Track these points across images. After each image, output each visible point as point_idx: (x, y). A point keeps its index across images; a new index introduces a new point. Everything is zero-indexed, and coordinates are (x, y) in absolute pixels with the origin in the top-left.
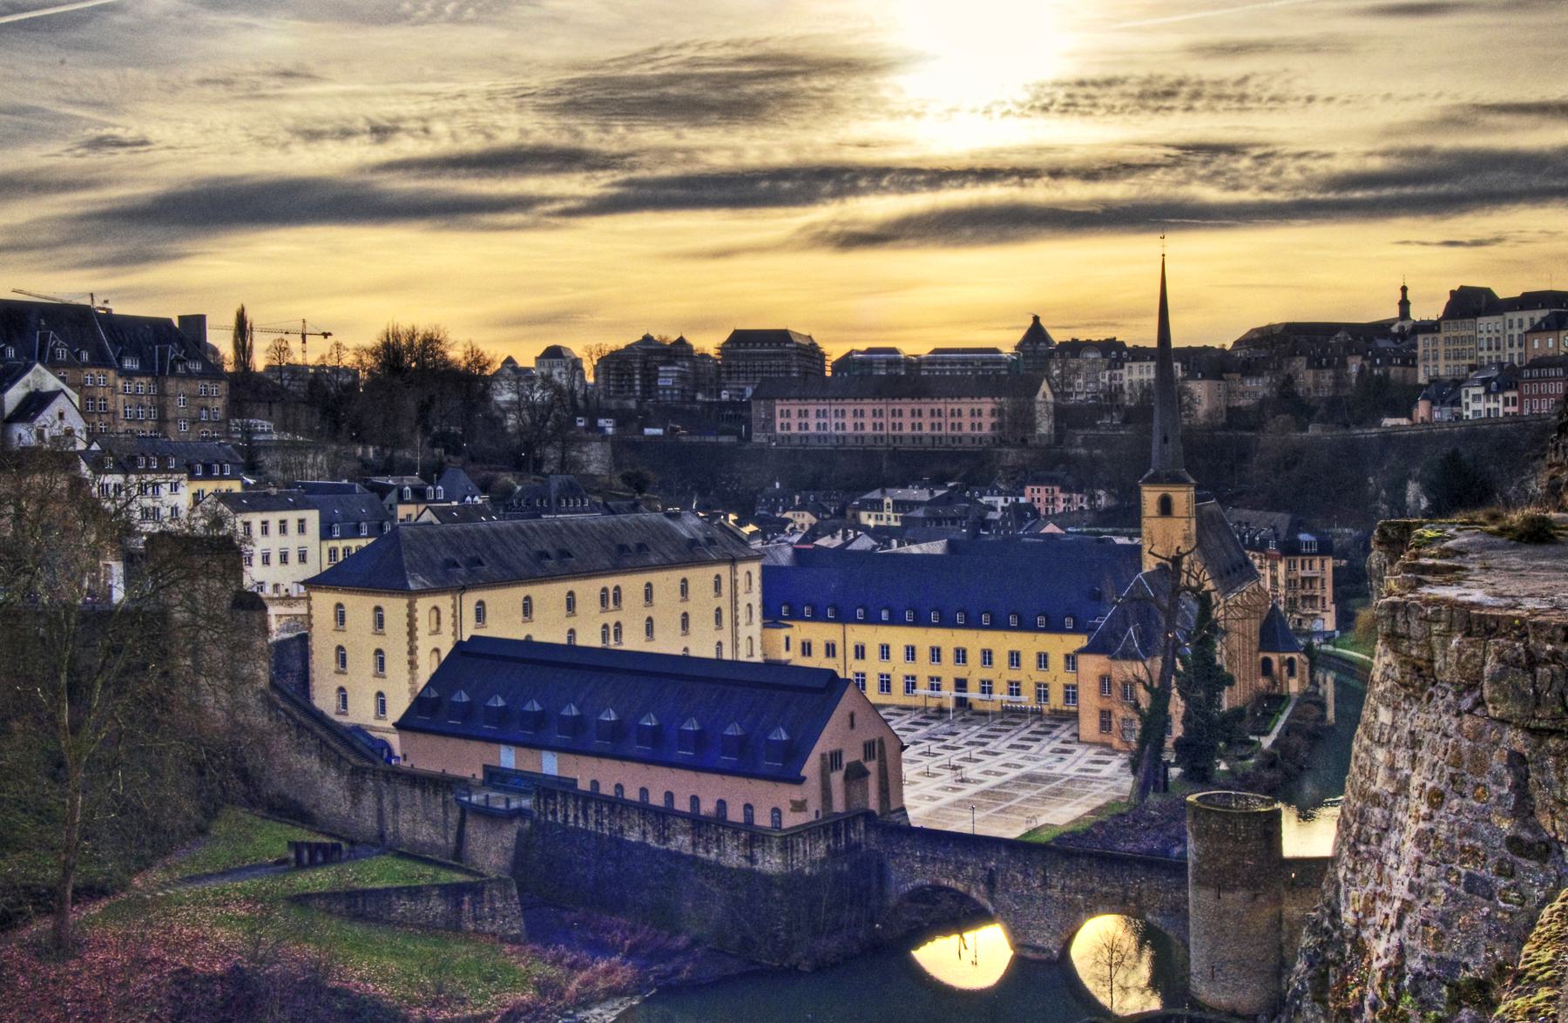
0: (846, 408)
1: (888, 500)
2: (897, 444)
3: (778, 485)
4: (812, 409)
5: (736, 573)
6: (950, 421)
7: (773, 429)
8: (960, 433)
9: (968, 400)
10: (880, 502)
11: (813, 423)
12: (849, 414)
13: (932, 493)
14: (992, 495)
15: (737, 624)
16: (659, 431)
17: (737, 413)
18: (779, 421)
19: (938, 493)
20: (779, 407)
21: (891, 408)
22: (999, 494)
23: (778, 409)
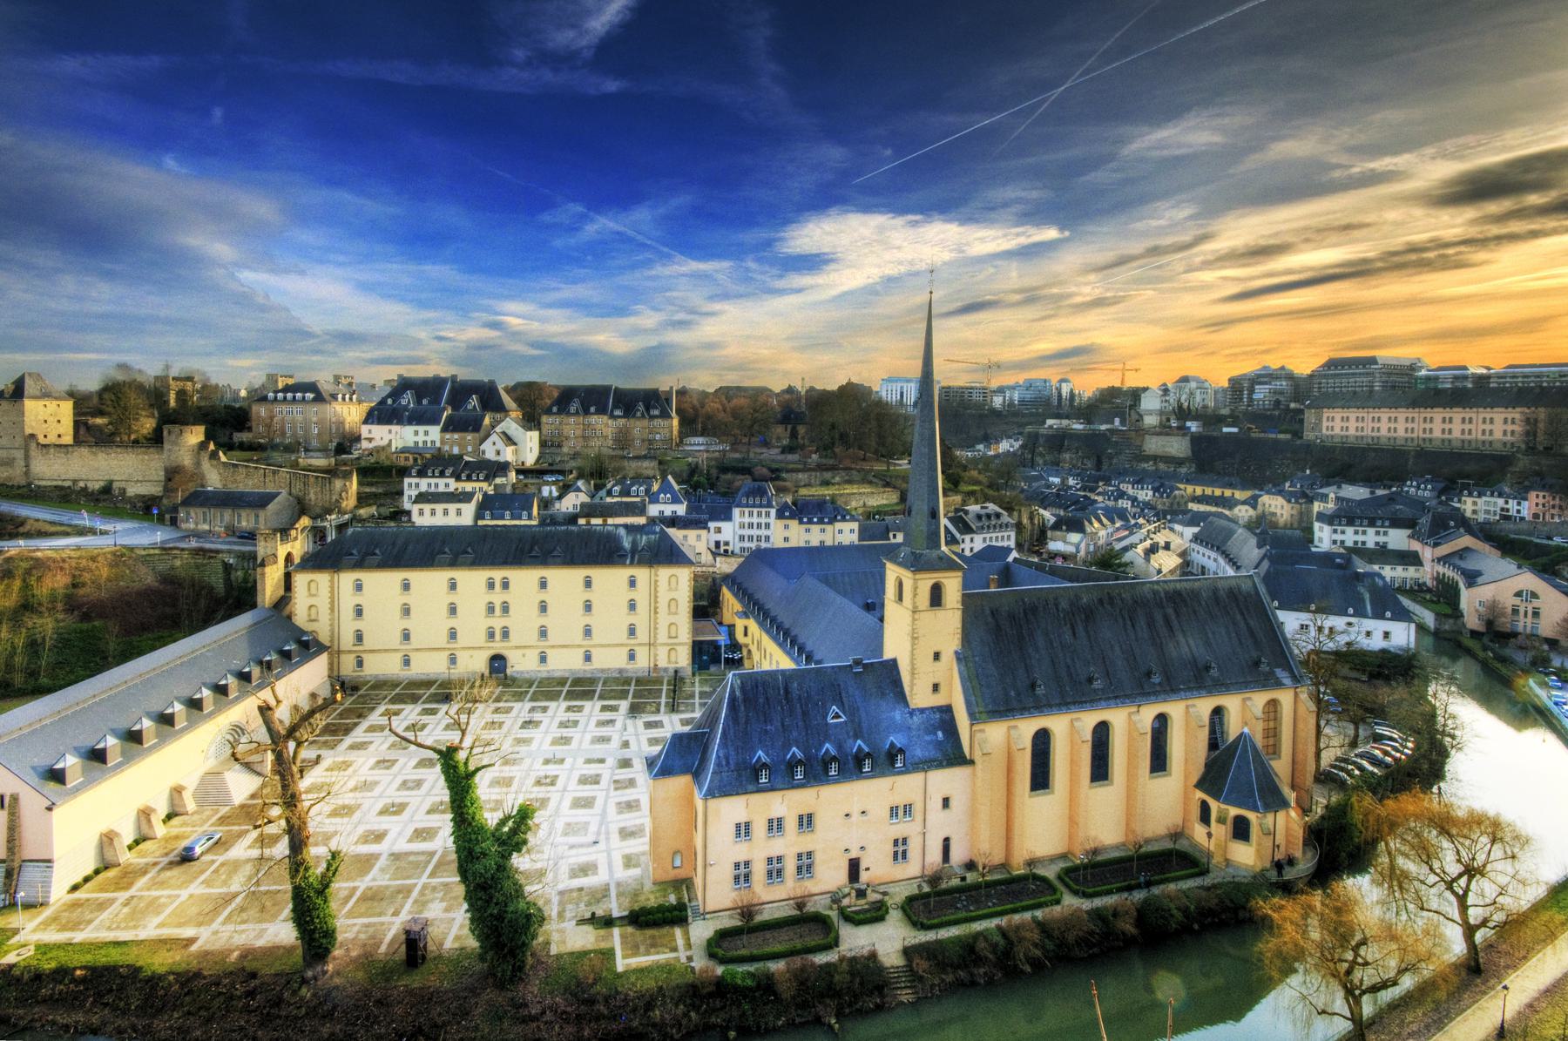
0: (1350, 415)
1: (1332, 496)
2: (1427, 444)
3: (1308, 472)
4: (1353, 416)
5: (656, 575)
6: (1423, 426)
7: (1321, 430)
8: (1491, 438)
9: (1441, 410)
10: (1327, 496)
11: (1352, 425)
12: (1338, 420)
13: (1372, 493)
14: (1492, 495)
15: (656, 613)
16: (1235, 430)
17: (1296, 418)
18: (1325, 424)
19: (1380, 492)
20: (1327, 413)
21: (1371, 415)
22: (1500, 495)
23: (1325, 416)
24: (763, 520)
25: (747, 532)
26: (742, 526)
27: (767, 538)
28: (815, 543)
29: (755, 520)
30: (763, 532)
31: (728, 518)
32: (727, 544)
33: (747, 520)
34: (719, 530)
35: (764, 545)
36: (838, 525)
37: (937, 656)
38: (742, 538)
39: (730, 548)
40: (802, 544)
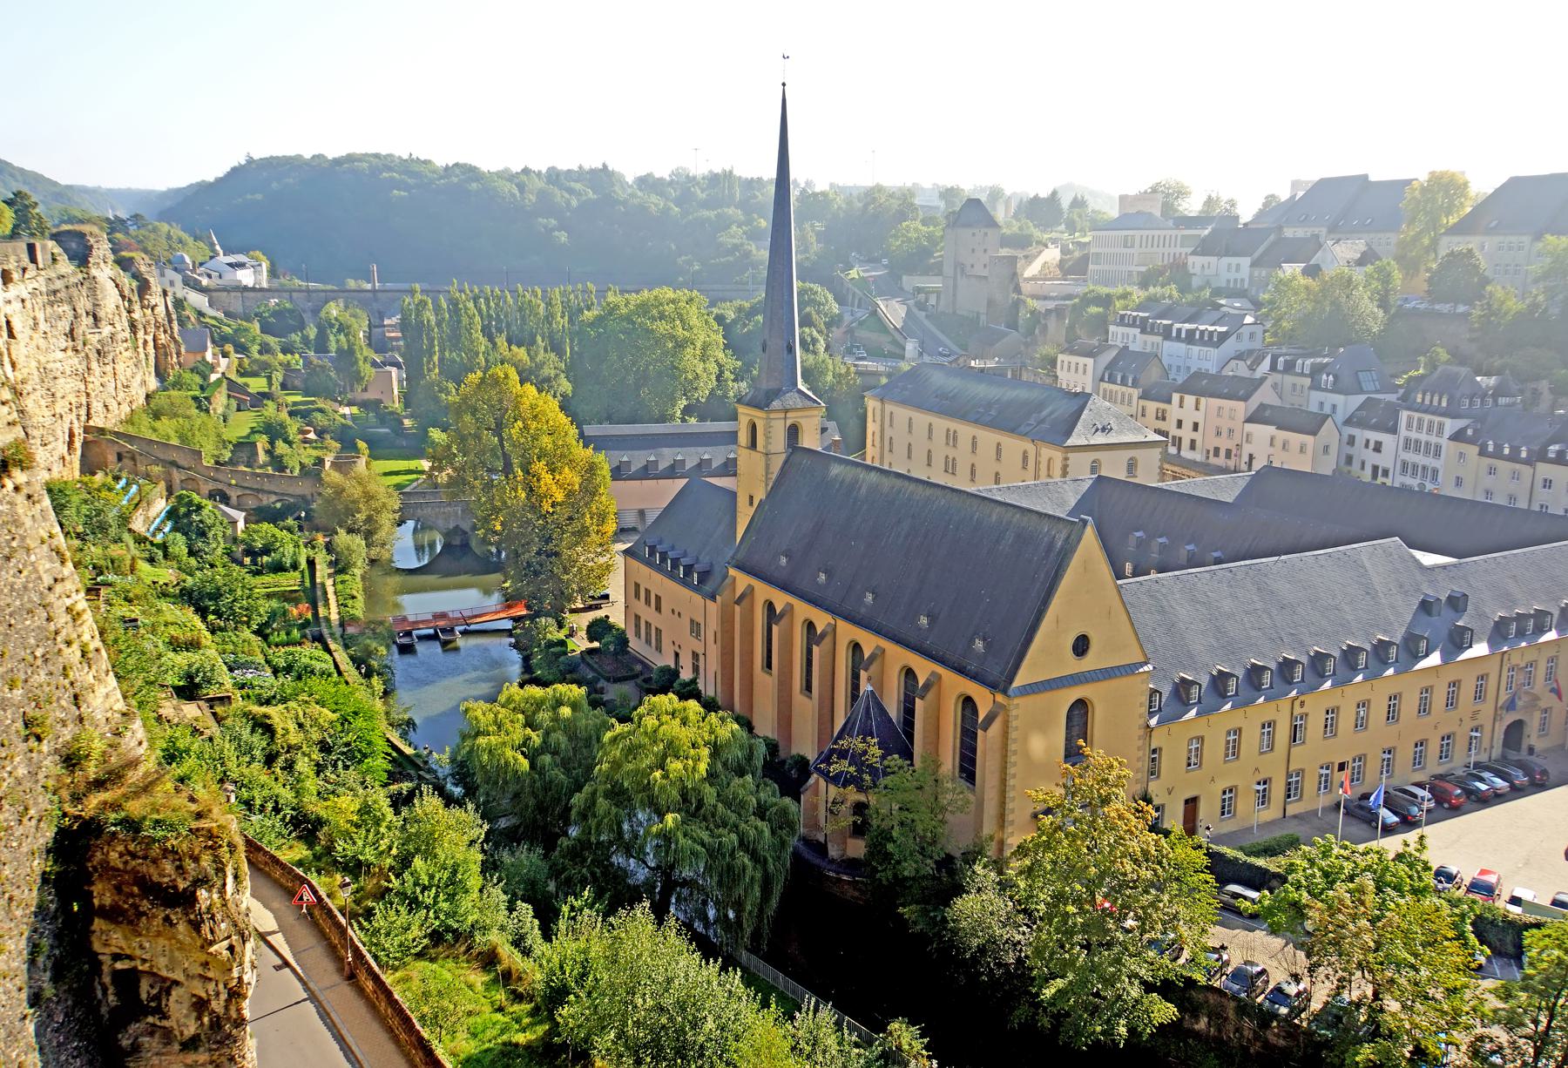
24: (1433, 439)
25: (1411, 457)
26: (1407, 446)
27: (1435, 472)
28: (1500, 500)
29: (1423, 437)
30: (1430, 462)
31: (1393, 430)
32: (1386, 473)
33: (1414, 435)
34: (1378, 448)
35: (1429, 486)
36: (1544, 470)
37: (751, 498)
38: (1405, 464)
39: (1389, 482)
40: (1481, 498)
